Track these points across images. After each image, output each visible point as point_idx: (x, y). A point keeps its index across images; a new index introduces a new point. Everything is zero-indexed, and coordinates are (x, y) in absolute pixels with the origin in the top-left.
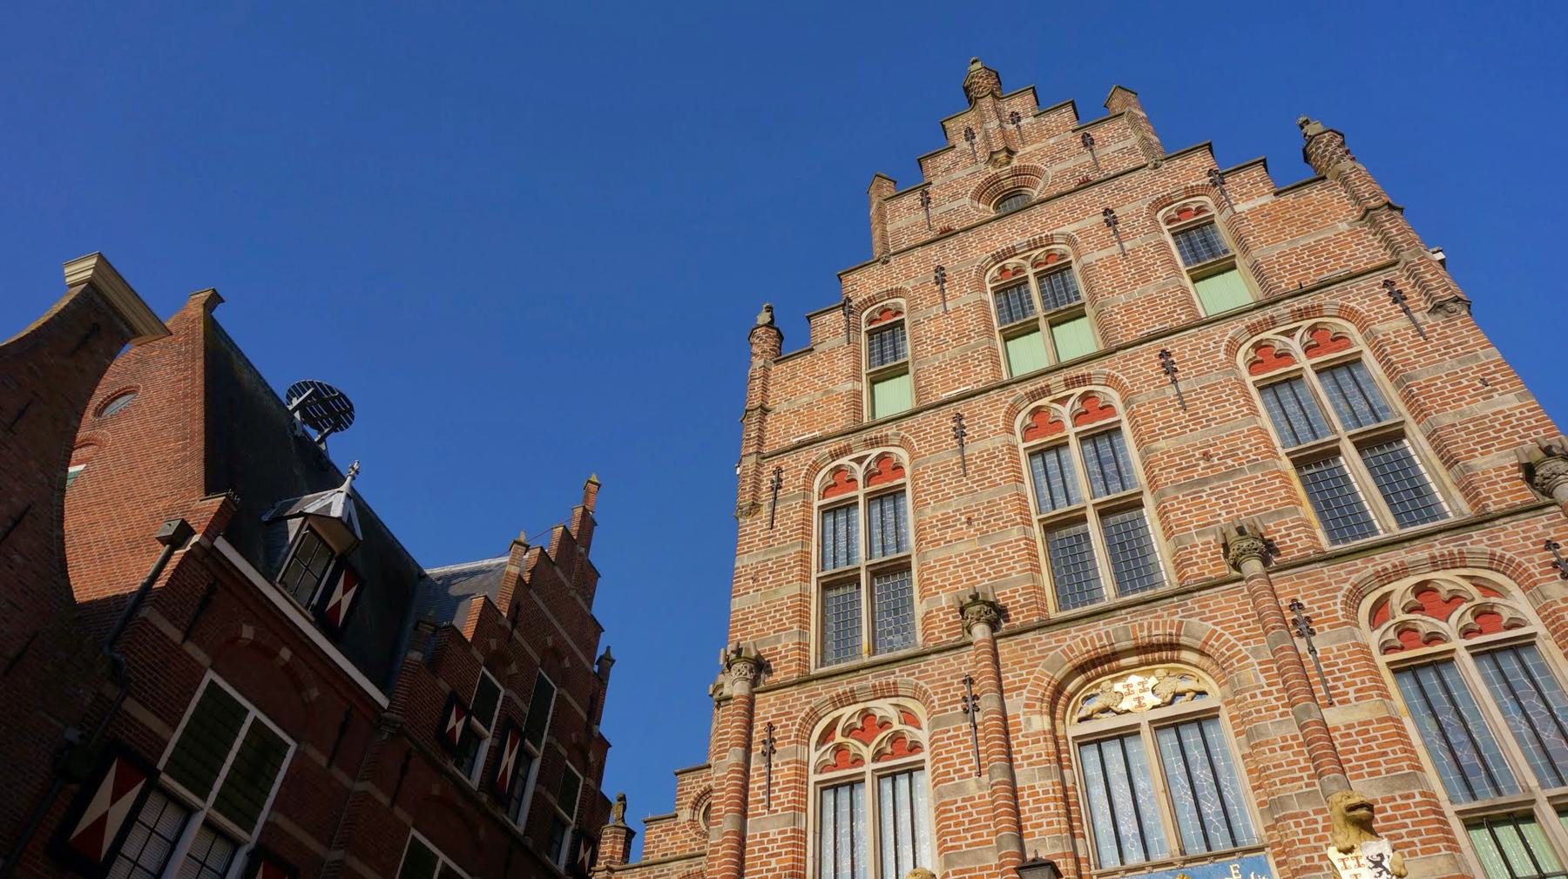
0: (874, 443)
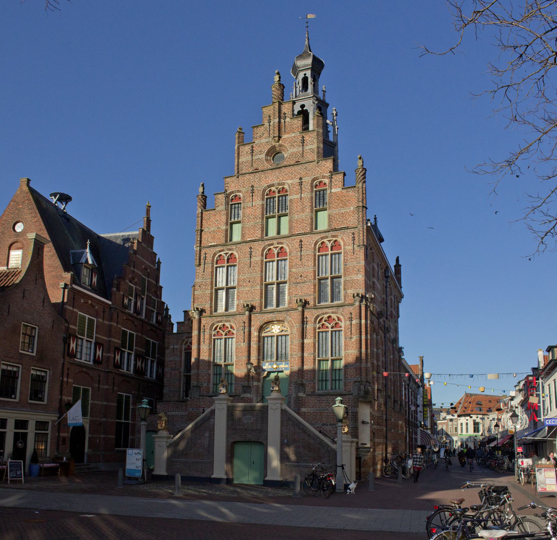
0: (230, 250)
